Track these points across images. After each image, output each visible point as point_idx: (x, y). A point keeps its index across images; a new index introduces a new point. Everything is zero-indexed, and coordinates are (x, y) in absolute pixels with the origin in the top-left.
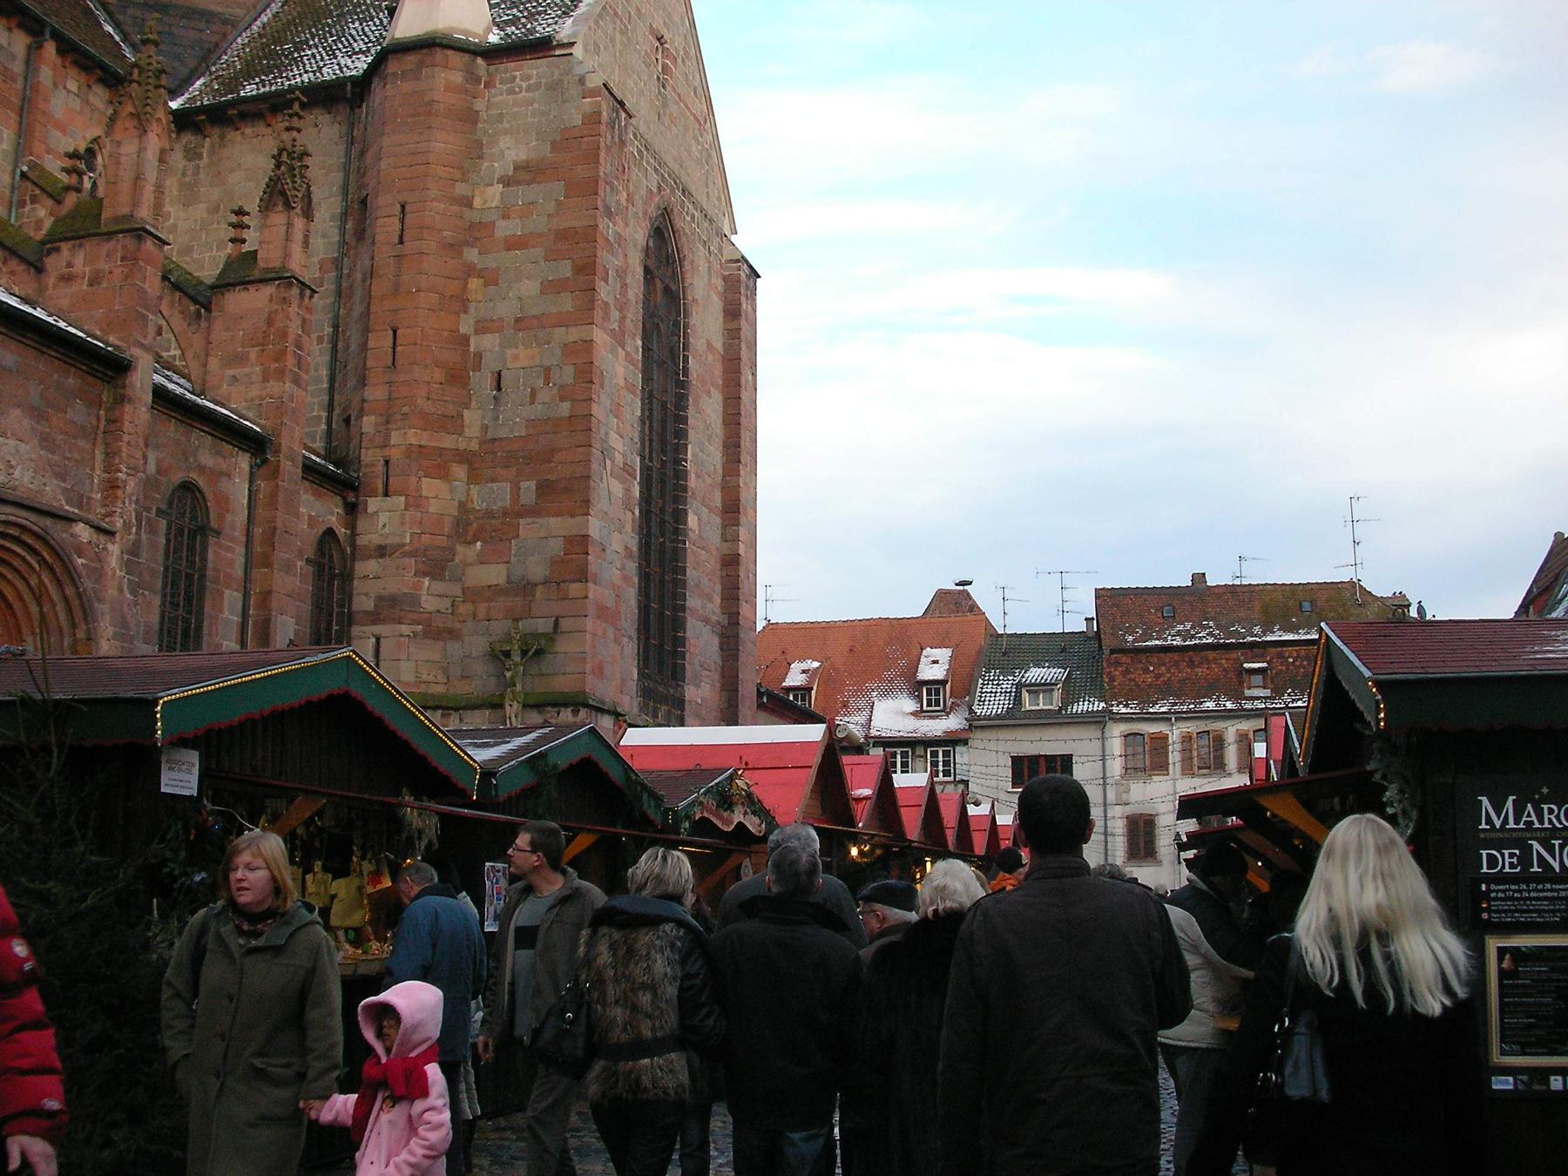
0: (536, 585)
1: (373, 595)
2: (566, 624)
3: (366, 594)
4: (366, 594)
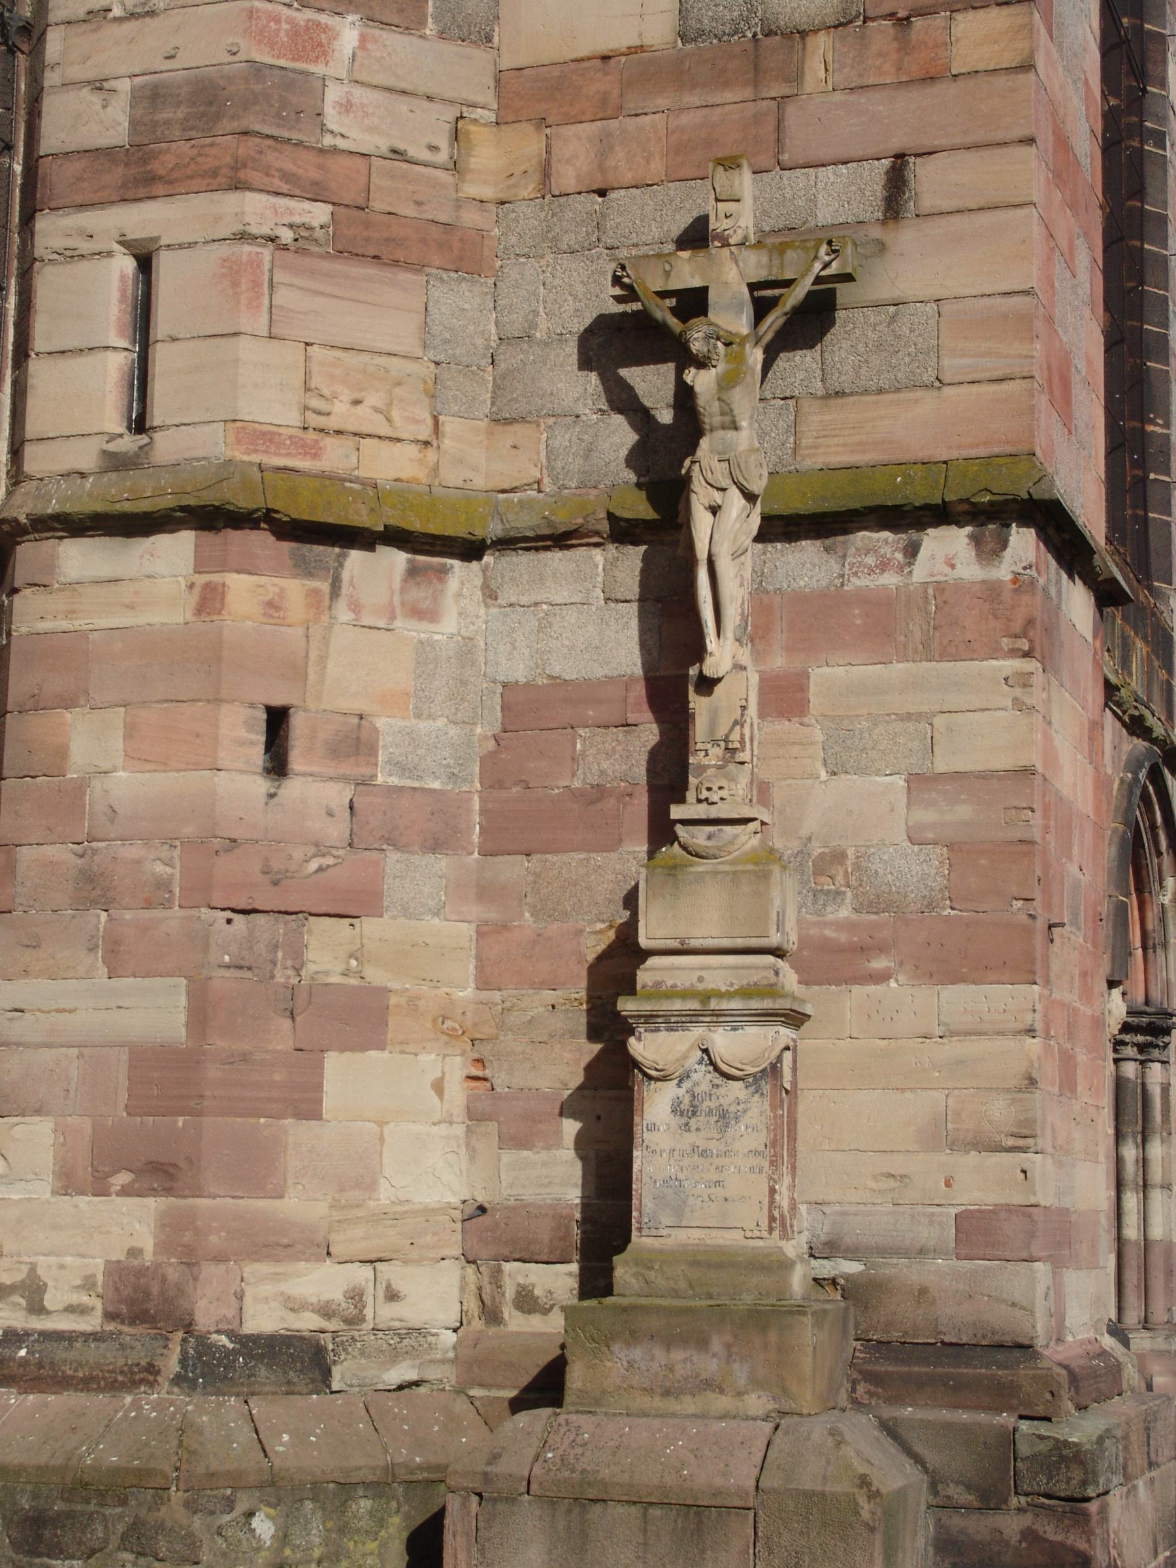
0: (803, 34)
1: (125, 86)
3: (98, 86)
4: (98, 86)
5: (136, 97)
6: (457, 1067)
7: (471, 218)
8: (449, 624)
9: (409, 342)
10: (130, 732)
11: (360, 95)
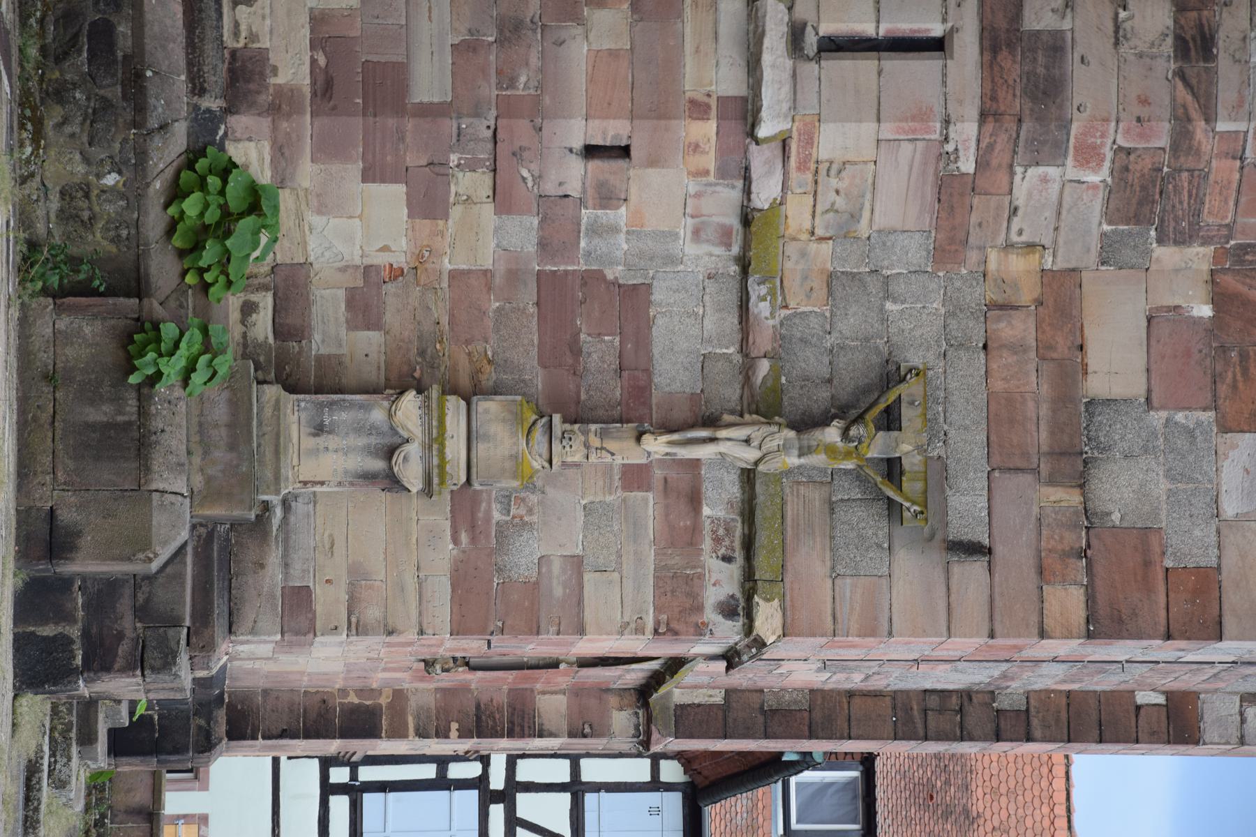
0: (1082, 486)
1: (1066, 25)
2: (971, 572)
5: (1057, 35)
6: (400, 259)
7: (973, 256)
8: (691, 249)
9: (881, 221)
10: (614, 54)
11: (1055, 188)
